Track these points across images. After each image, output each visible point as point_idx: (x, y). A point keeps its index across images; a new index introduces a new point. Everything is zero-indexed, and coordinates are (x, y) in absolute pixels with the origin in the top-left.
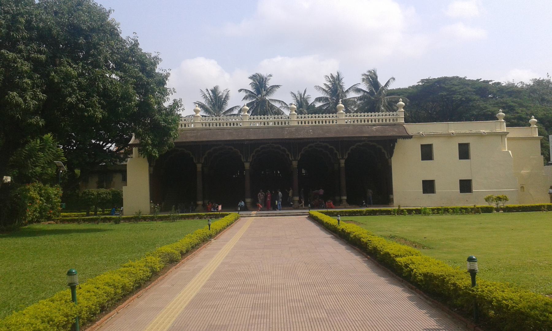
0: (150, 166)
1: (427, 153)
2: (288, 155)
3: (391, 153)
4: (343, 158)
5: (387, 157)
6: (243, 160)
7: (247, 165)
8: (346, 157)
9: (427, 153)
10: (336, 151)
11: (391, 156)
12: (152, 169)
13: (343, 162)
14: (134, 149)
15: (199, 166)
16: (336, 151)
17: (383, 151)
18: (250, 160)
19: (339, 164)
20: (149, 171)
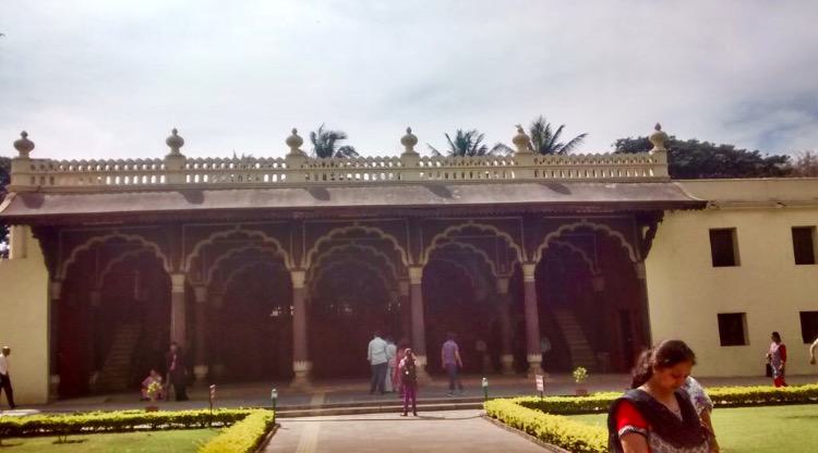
0: (52, 279)
1: (724, 249)
2: (396, 257)
3: (644, 247)
4: (530, 262)
5: (633, 258)
6: (288, 266)
7: (298, 279)
8: (538, 258)
9: (724, 249)
10: (512, 245)
11: (644, 255)
12: (57, 287)
13: (529, 272)
14: (11, 229)
15: (178, 283)
16: (512, 245)
17: (624, 243)
18: (306, 264)
19: (519, 273)
20: (50, 292)
